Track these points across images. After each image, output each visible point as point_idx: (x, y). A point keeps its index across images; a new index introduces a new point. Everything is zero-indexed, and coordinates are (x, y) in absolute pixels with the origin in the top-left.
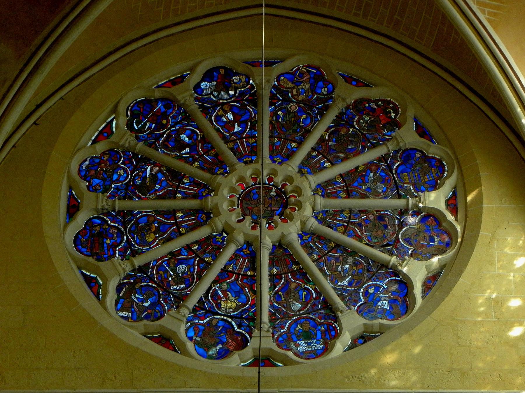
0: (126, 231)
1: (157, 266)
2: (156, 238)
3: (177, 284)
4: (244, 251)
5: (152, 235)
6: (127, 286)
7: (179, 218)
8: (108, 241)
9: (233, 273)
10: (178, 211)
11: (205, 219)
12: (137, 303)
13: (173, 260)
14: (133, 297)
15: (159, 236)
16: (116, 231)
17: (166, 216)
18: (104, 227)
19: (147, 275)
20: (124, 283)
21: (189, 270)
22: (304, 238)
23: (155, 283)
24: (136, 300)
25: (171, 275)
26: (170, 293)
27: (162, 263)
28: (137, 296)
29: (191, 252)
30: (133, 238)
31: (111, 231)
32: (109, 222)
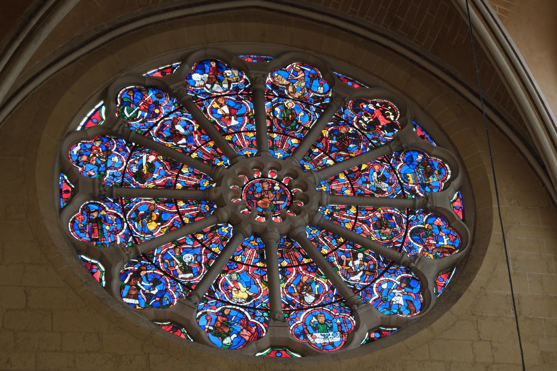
0: (126, 219)
1: (163, 255)
2: (159, 226)
3: (185, 272)
4: (252, 242)
5: (154, 223)
6: (131, 274)
7: (181, 208)
8: (107, 228)
9: (242, 263)
10: (180, 200)
11: (208, 209)
12: (143, 290)
13: (178, 249)
14: (139, 285)
15: (162, 225)
16: (115, 218)
17: (167, 205)
18: (102, 213)
19: (152, 262)
20: (127, 270)
21: (196, 259)
22: (312, 233)
23: (161, 271)
24: (142, 287)
25: (177, 264)
26: (178, 281)
27: (166, 252)
28: (143, 283)
29: (196, 242)
30: (134, 226)
31: (110, 218)
32: (107, 209)
